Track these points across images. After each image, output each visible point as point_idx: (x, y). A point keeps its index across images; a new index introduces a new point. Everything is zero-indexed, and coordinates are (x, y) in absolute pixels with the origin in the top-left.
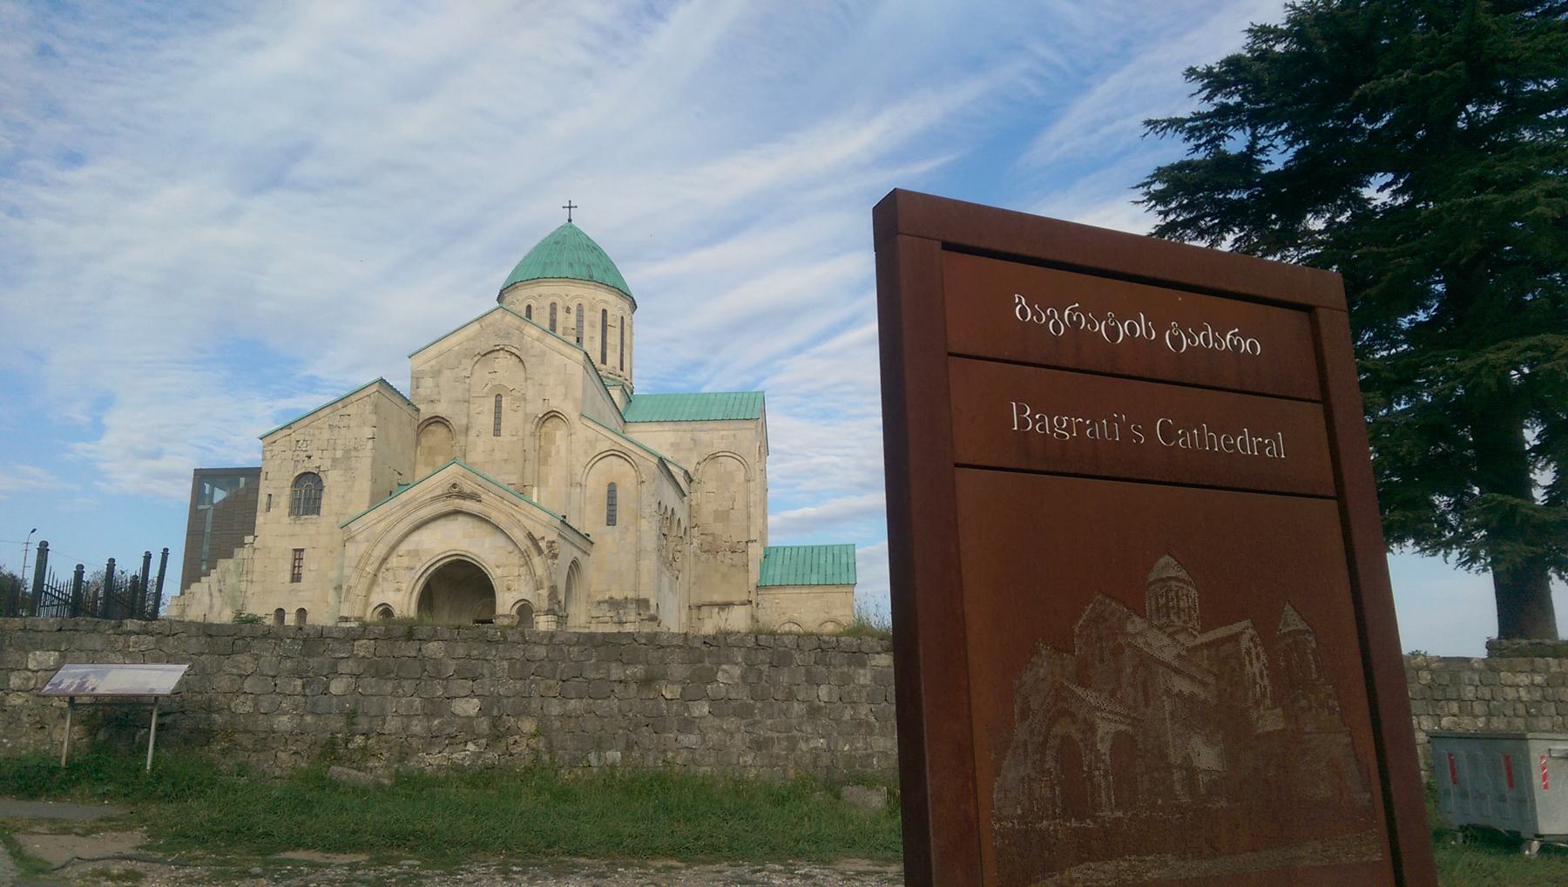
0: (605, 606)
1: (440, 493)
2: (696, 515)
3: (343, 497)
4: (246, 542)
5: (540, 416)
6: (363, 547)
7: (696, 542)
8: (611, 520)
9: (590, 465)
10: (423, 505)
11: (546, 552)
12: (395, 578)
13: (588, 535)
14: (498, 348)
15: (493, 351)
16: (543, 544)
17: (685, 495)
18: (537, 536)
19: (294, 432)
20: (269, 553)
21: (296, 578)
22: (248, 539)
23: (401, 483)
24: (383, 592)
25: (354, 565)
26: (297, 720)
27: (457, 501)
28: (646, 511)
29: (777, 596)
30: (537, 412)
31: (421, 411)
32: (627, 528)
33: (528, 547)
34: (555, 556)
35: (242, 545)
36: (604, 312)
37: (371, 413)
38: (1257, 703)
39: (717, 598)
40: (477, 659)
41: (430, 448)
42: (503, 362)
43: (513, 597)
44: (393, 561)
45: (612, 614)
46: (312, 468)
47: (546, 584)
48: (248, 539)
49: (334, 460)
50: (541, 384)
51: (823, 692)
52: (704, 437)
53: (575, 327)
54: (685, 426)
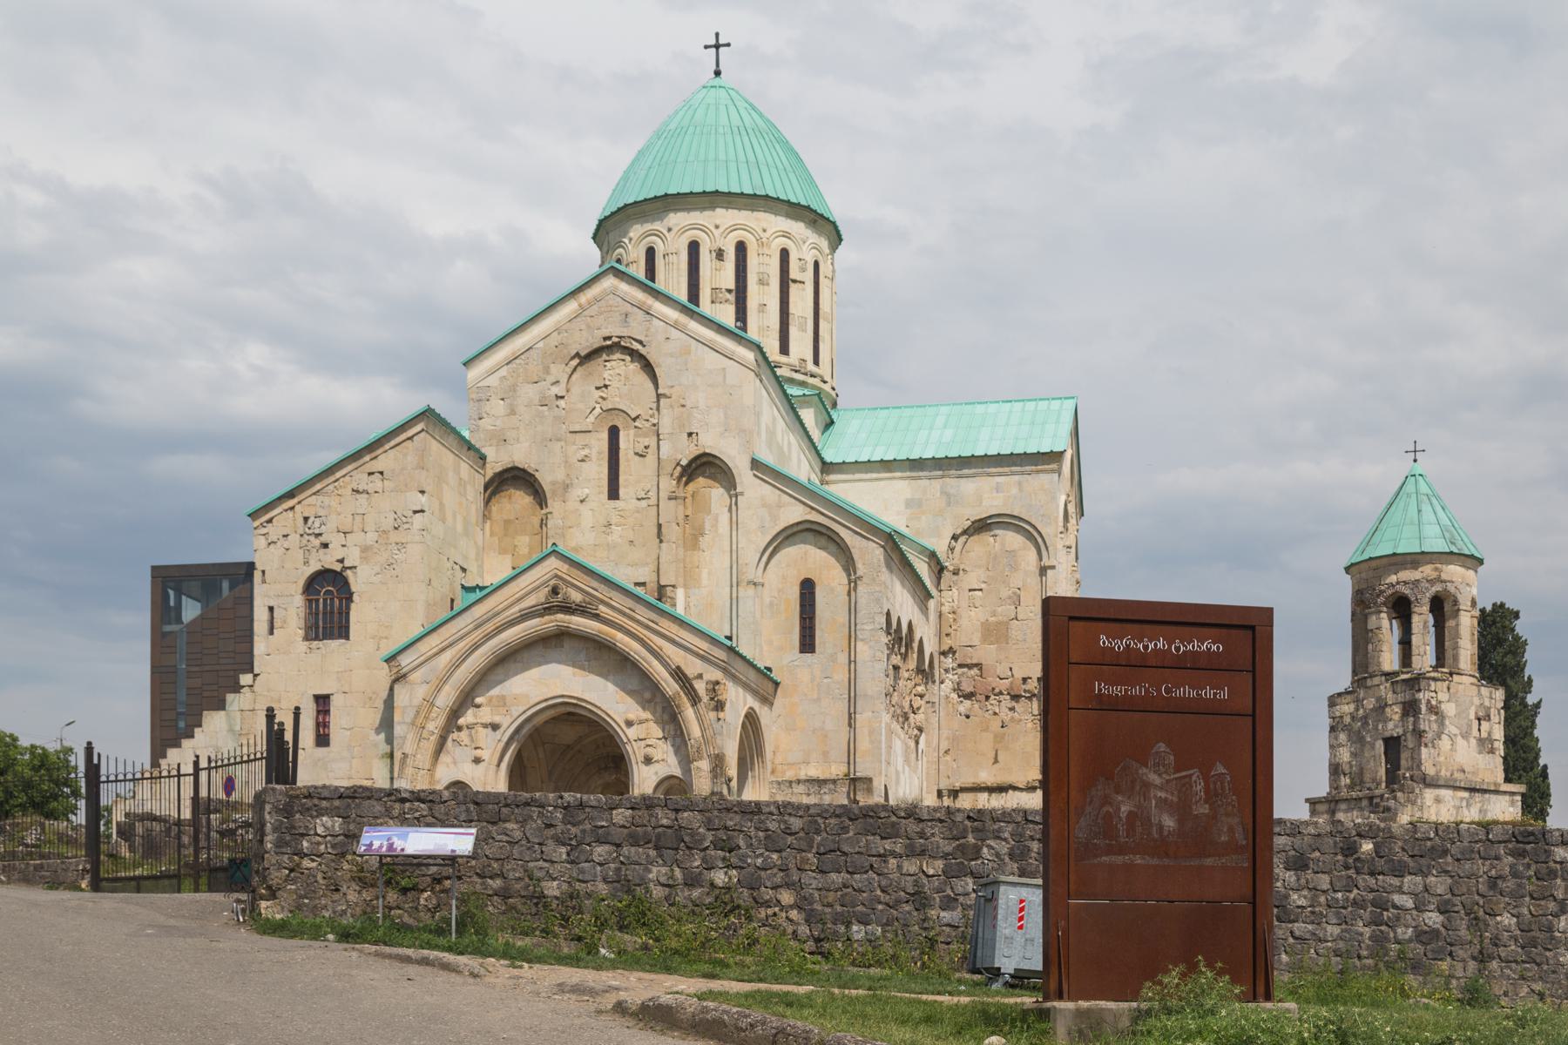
1: (533, 603)
2: (950, 630)
5: (684, 462)
6: (421, 692)
8: (807, 644)
12: (472, 741)
13: (769, 669)
16: (700, 687)
17: (929, 596)
18: (690, 672)
23: (466, 585)
24: (455, 763)
25: (408, 720)
26: (565, 886)
27: (560, 616)
28: (866, 627)
30: (679, 457)
31: (488, 460)
34: (719, 706)
38: (1196, 802)
40: (733, 830)
41: (507, 522)
42: (619, 370)
43: (656, 773)
46: (332, 563)
49: (365, 549)
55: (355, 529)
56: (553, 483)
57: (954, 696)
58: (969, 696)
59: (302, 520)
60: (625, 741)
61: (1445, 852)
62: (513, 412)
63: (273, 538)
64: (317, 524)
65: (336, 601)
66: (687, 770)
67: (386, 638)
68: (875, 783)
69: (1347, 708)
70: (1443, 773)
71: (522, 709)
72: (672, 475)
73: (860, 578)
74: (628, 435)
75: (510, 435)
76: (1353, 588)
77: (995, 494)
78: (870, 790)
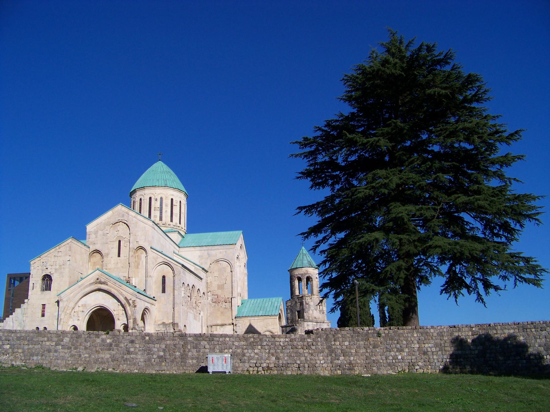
0: (161, 326)
2: (210, 287)
6: (65, 304)
7: (210, 298)
8: (164, 291)
10: (87, 286)
11: (132, 304)
13: (154, 297)
14: (119, 221)
15: (117, 222)
16: (131, 302)
18: (129, 298)
20: (33, 306)
21: (43, 315)
22: (26, 301)
24: (73, 321)
29: (244, 321)
32: (170, 294)
33: (125, 303)
34: (135, 306)
35: (24, 303)
36: (172, 200)
39: (219, 322)
41: (94, 263)
42: (122, 226)
44: (77, 309)
45: (164, 329)
47: (132, 317)
48: (26, 301)
49: (56, 269)
51: (89, 344)
52: (213, 252)
53: (159, 207)
54: (205, 248)
57: (211, 302)
58: (214, 302)
59: (42, 263)
60: (113, 315)
61: (164, 339)
62: (96, 237)
63: (35, 267)
65: (49, 282)
68: (179, 324)
70: (310, 319)
71: (89, 307)
78: (178, 326)
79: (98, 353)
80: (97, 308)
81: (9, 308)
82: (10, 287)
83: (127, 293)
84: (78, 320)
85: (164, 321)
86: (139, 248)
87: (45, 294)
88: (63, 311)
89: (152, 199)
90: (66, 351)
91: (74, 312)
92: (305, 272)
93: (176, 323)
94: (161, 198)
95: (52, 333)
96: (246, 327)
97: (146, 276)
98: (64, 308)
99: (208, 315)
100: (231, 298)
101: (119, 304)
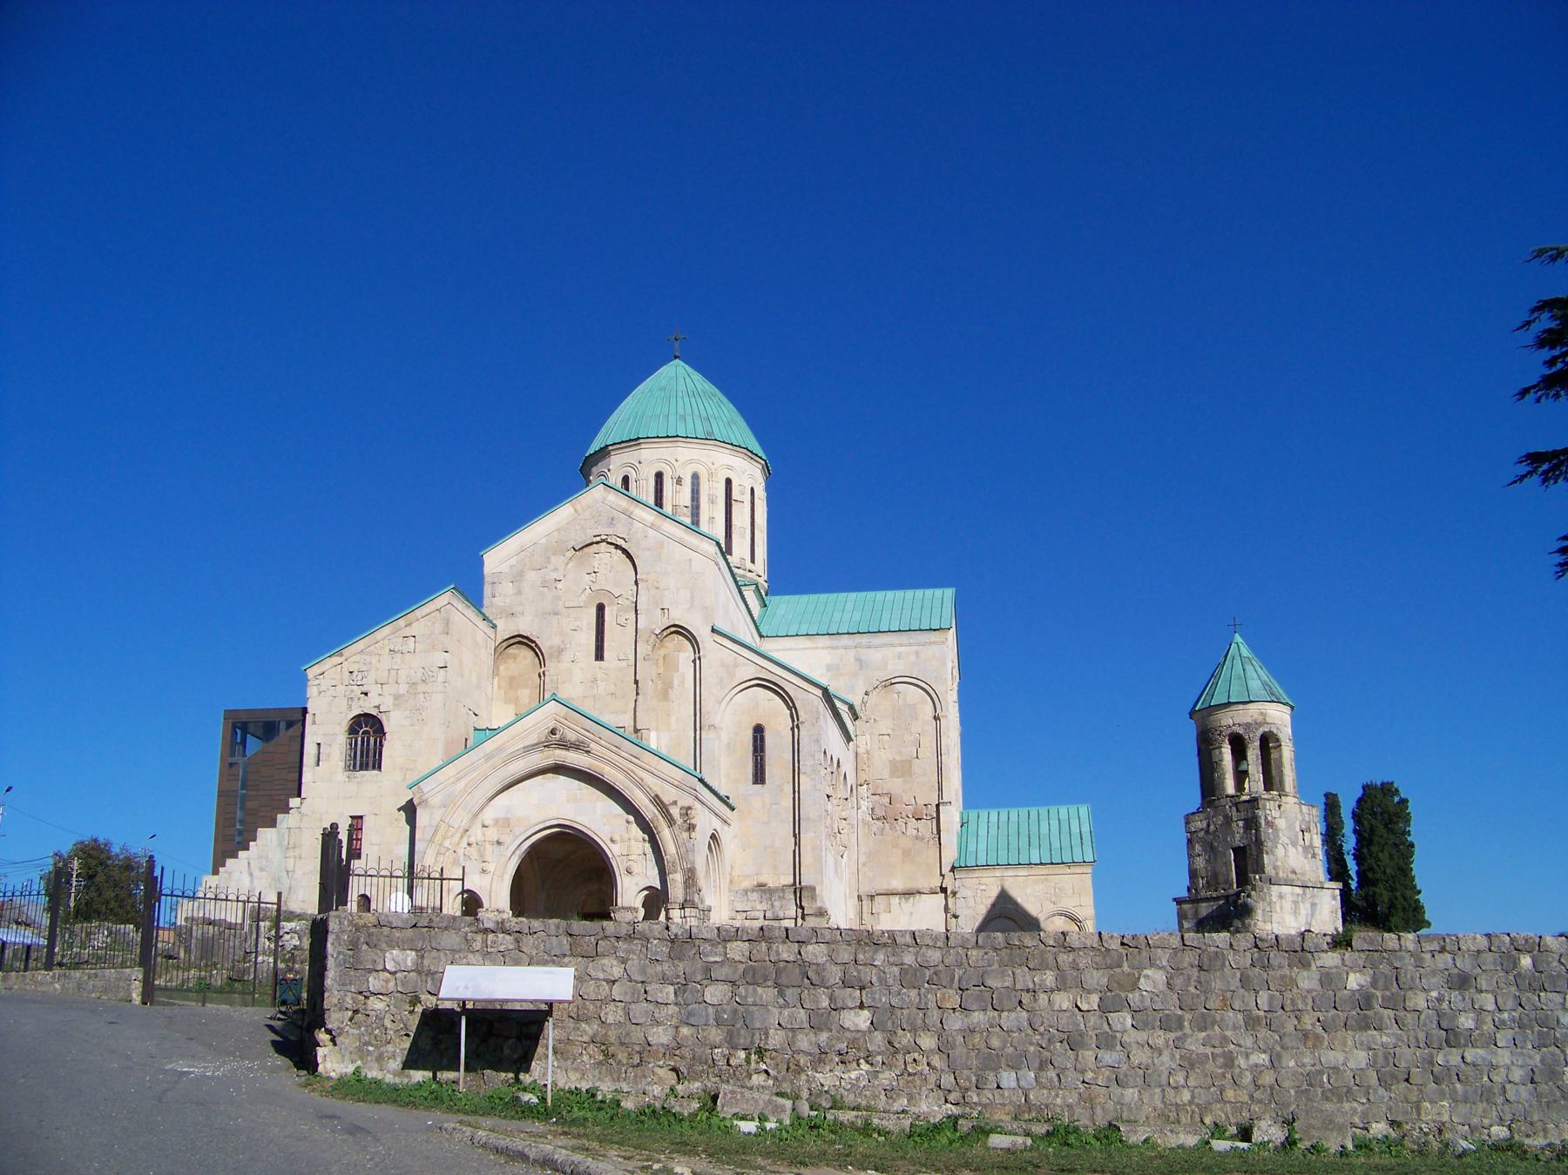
0: (755, 896)
2: (864, 767)
3: (410, 746)
4: (291, 806)
6: (438, 815)
7: (865, 805)
8: (759, 777)
9: (727, 699)
10: (515, 756)
11: (679, 821)
13: (728, 798)
14: (598, 539)
15: (591, 544)
16: (675, 811)
18: (666, 799)
19: (346, 660)
22: (294, 802)
27: (558, 752)
32: (780, 788)
34: (691, 828)
35: (286, 809)
36: (729, 482)
37: (441, 633)
39: (898, 884)
41: (512, 679)
42: (608, 559)
43: (637, 884)
44: (477, 834)
45: (764, 906)
48: (294, 802)
49: (397, 697)
50: (657, 588)
54: (846, 640)
55: (391, 681)
56: (551, 648)
58: (878, 819)
60: (610, 856)
62: (519, 593)
63: (322, 688)
64: (360, 678)
66: (663, 880)
67: (412, 770)
69: (1199, 824)
72: (648, 642)
73: (802, 723)
74: (612, 611)
75: (515, 609)
76: (1197, 728)
77: (897, 661)
78: (813, 897)
79: (1314, 1046)
80: (549, 831)
81: (235, 826)
82: (233, 754)
83: (659, 782)
84: (484, 871)
85: (763, 879)
86: (668, 631)
87: (359, 780)
88: (431, 841)
89: (665, 477)
90: (1159, 1038)
91: (469, 844)
92: (1256, 716)
93: (806, 887)
94: (695, 477)
95: (1076, 944)
96: (990, 902)
97: (698, 727)
98: (436, 832)
99: (863, 859)
100: (938, 806)
101: (631, 818)
